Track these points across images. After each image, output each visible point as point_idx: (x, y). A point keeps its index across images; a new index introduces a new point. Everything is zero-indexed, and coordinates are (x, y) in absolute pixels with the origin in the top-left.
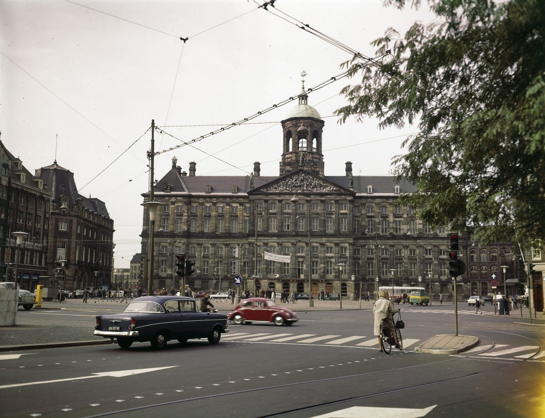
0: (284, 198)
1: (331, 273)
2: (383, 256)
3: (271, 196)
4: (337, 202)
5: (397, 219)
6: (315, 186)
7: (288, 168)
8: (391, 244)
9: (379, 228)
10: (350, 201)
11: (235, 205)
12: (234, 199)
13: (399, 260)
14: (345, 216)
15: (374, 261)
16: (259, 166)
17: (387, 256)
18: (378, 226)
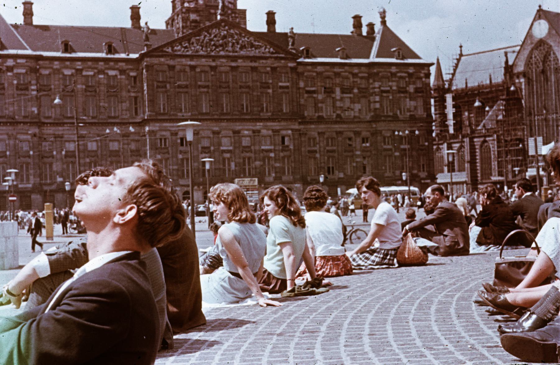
0: (198, 63)
1: (269, 174)
2: (327, 148)
3: (179, 60)
4: (274, 69)
5: (345, 95)
6: (245, 45)
7: (193, 16)
8: (339, 130)
9: (322, 107)
10: (293, 69)
11: (112, 73)
12: (112, 64)
13: (350, 152)
14: (286, 90)
15: (318, 155)
16: (139, 12)
17: (335, 148)
18: (320, 105)
